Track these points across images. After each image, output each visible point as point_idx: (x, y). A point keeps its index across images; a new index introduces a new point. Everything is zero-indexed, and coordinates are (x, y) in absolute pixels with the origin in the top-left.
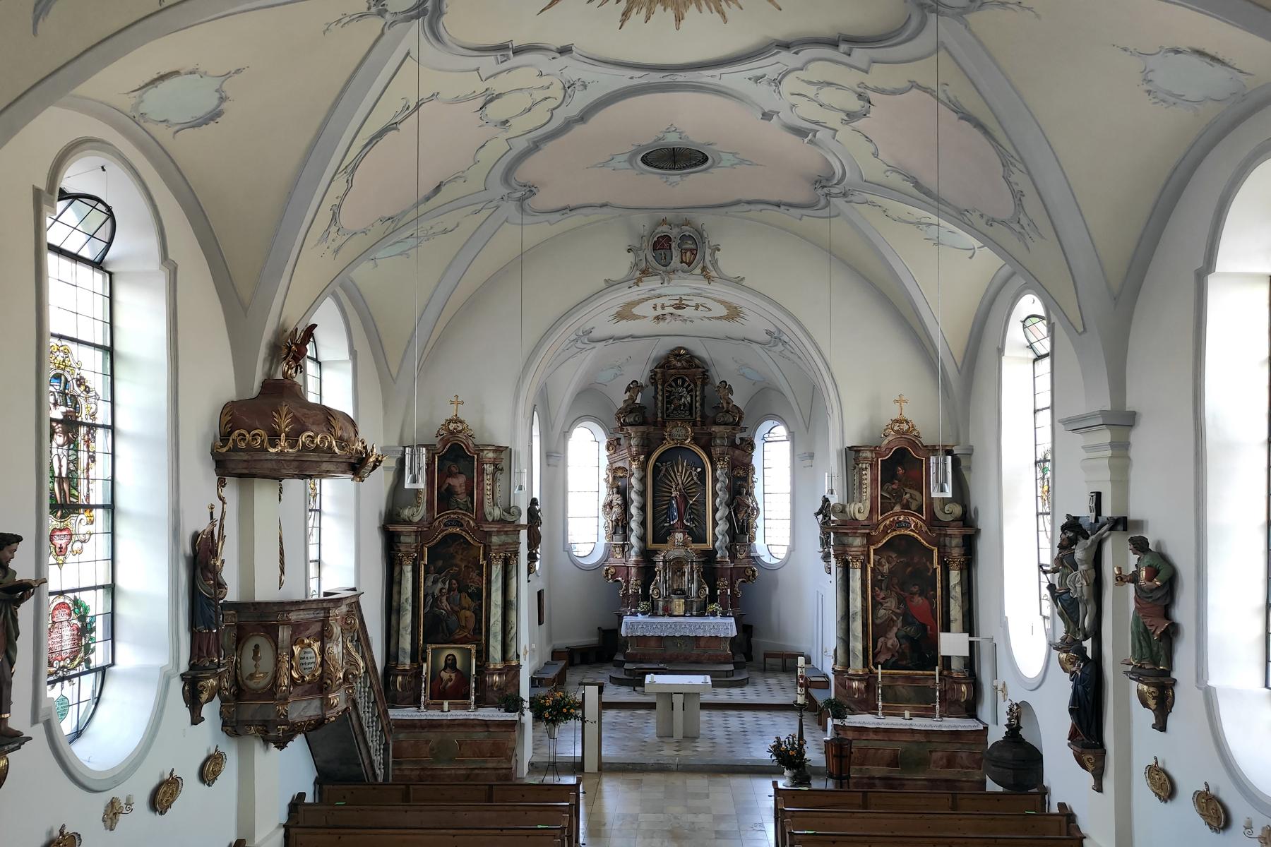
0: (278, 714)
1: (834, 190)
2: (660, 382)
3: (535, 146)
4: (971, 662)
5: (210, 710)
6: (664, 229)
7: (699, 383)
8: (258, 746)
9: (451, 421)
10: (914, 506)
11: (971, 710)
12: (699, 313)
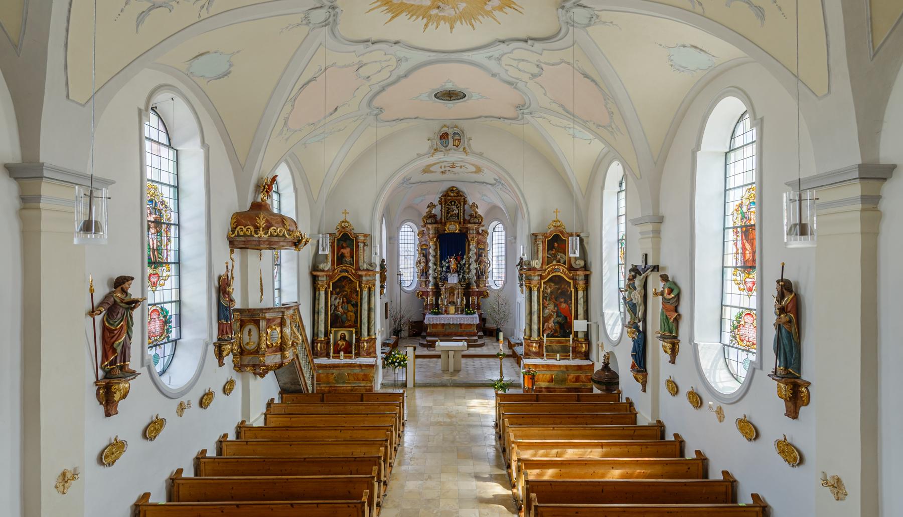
1: (526, 111)
3: (383, 89)
4: (587, 335)
5: (228, 360)
6: (445, 130)
8: (251, 375)
10: (562, 261)
11: (587, 355)
12: (463, 170)
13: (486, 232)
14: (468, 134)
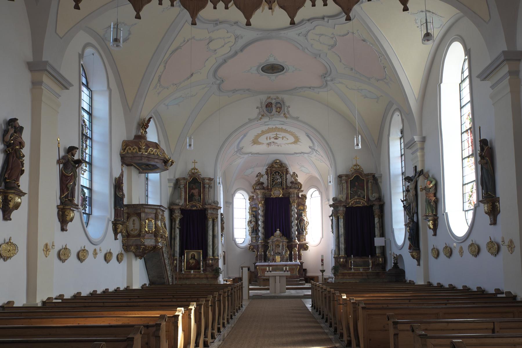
0: (142, 242)
2: (269, 173)
3: (225, 61)
6: (269, 101)
7: (285, 173)
9: (193, 169)
10: (362, 196)
12: (284, 141)
13: (304, 197)
14: (287, 104)
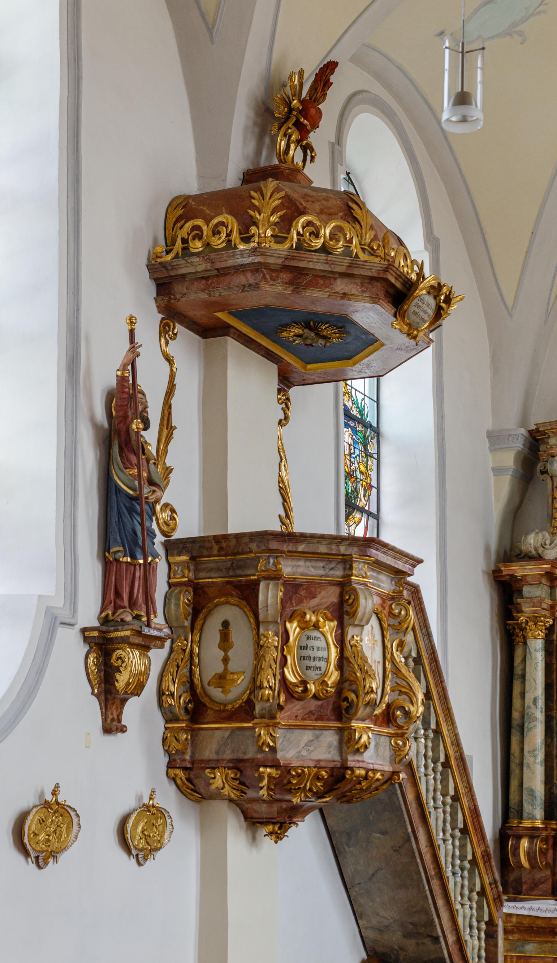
5: (142, 713)
